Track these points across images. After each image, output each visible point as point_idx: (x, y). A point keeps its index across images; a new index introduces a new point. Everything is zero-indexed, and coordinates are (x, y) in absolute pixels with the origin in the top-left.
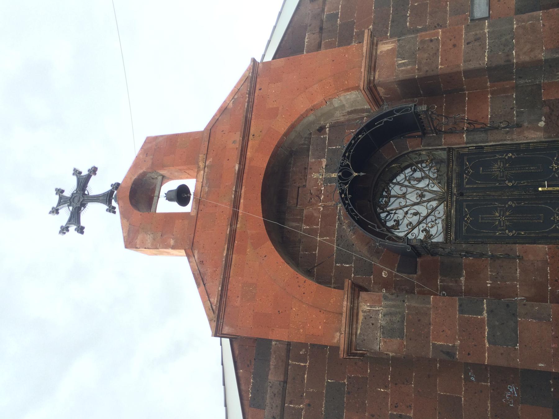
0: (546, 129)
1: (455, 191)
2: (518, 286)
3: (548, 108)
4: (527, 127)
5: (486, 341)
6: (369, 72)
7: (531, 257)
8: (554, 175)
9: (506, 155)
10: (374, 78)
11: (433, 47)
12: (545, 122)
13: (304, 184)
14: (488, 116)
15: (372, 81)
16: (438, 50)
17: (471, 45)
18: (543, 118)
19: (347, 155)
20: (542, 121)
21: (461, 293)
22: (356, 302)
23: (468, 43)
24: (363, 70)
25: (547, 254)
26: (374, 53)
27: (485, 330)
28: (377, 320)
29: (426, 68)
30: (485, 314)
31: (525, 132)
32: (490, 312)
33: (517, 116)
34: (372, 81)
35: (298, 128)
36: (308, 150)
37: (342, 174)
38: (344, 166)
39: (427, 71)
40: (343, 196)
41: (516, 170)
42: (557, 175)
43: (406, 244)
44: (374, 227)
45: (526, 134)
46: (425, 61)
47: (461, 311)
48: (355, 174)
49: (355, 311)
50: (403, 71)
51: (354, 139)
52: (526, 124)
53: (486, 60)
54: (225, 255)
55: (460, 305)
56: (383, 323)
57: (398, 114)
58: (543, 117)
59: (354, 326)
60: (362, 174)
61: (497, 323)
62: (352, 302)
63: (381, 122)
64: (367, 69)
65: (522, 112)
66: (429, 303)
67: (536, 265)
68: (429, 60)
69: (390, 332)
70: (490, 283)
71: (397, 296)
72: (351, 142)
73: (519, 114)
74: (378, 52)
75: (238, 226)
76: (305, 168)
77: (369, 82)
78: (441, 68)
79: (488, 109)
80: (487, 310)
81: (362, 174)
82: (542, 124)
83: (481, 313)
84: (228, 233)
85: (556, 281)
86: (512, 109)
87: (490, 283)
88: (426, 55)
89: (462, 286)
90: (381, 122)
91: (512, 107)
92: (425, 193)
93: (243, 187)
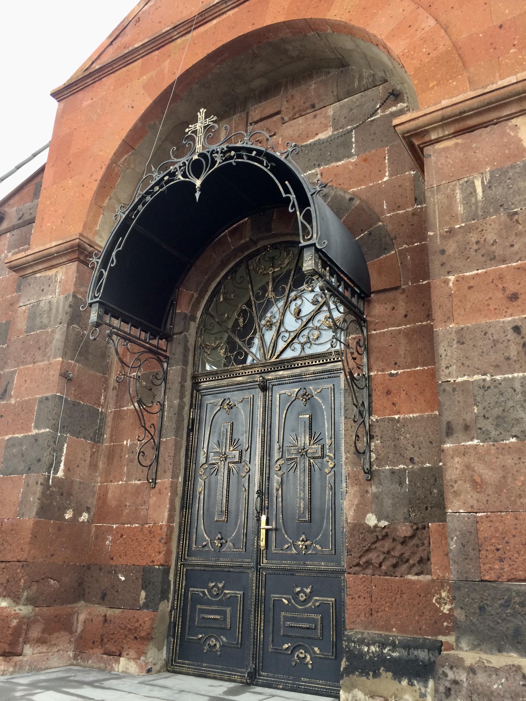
0: (358, 527)
1: (270, 376)
2: (120, 482)
3: (409, 534)
4: (367, 492)
5: (10, 436)
6: (445, 121)
7: (153, 500)
8: (287, 542)
9: (330, 458)
10: (438, 141)
11: (516, 247)
12: (376, 526)
13: (286, 119)
14: (399, 413)
15: (426, 139)
16: (504, 261)
17: (511, 335)
18: (383, 523)
19: (233, 153)
20: (379, 520)
21: (120, 406)
22: (64, 259)
23: (517, 329)
24: (445, 103)
25: (155, 524)
26: (506, 112)
27: (21, 433)
28: (46, 294)
29: (451, 247)
30: (34, 432)
31: (356, 488)
32: (36, 438)
33: (393, 472)
34: (426, 139)
35: (363, 44)
36: (349, 94)
37: (196, 160)
38: (213, 158)
39: (443, 252)
40: (166, 178)
41: (300, 476)
42: (286, 546)
43: (90, 301)
44: (119, 247)
45: (352, 490)
46: (474, 240)
47: (41, 401)
48: (198, 183)
49: (54, 262)
50: (451, 197)
51: (259, 152)
52: (373, 489)
53: (460, 380)
54: (136, 46)
55: (47, 399)
56: (42, 304)
57: (300, 218)
58: (386, 523)
59: (40, 267)
60: (197, 195)
61: (24, 448)
62: (60, 254)
63: (287, 191)
64: (448, 111)
65: (401, 483)
66: (54, 358)
67: (143, 507)
68: (475, 247)
69: (33, 315)
70: (127, 444)
71: (67, 313)
72: (250, 150)
73: (398, 477)
74: (514, 121)
75: (179, 41)
76: (313, 106)
77: (420, 132)
78: (446, 282)
79: (413, 412)
80: (38, 434)
81: (197, 195)
82: (371, 520)
83: (37, 427)
84: (164, 31)
85: (122, 536)
86: (411, 459)
87: (127, 444)
88: (490, 237)
89: (128, 406)
90: (287, 191)
91: (416, 459)
92: (274, 328)
93: (236, 10)
